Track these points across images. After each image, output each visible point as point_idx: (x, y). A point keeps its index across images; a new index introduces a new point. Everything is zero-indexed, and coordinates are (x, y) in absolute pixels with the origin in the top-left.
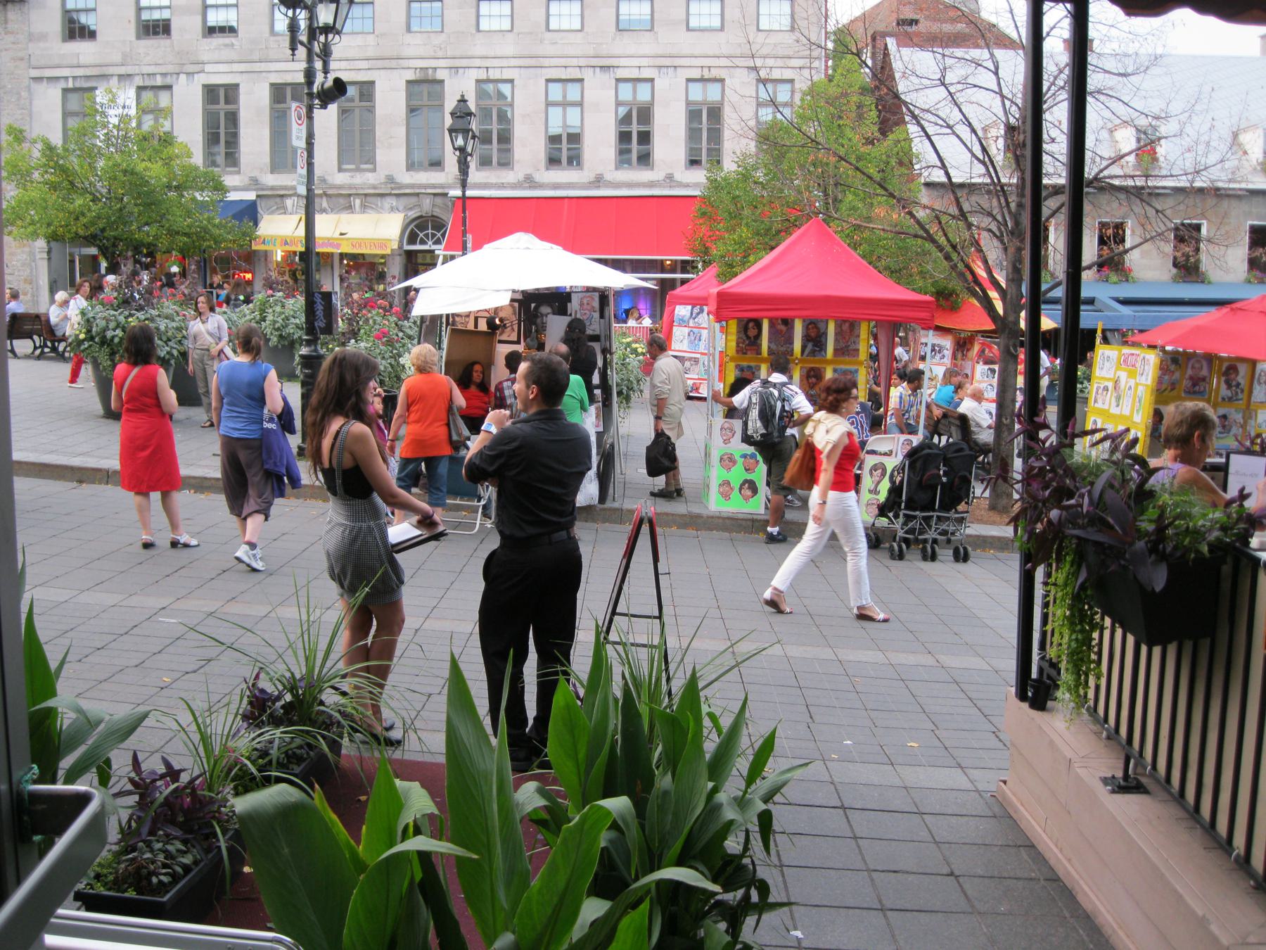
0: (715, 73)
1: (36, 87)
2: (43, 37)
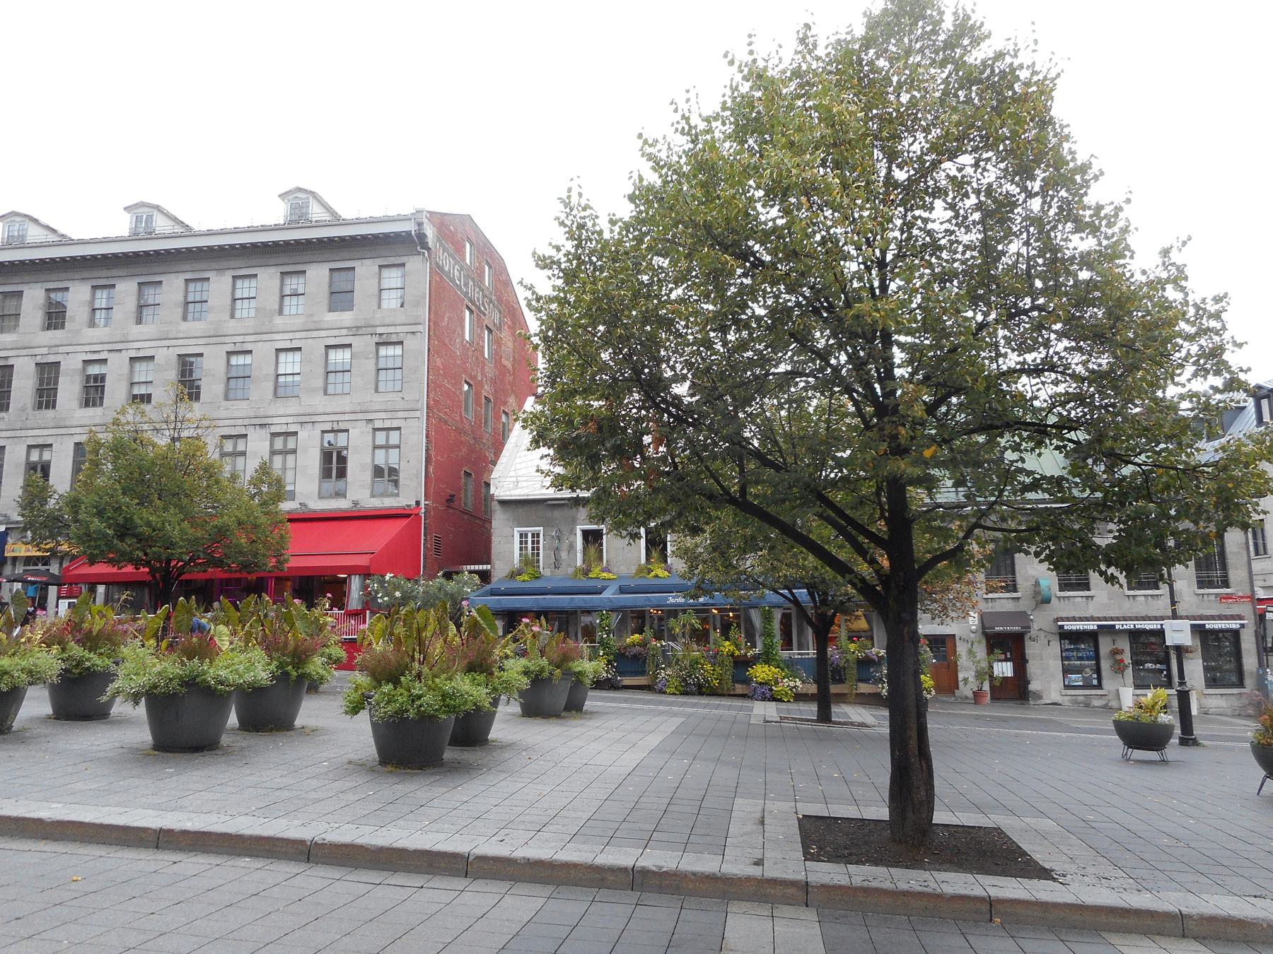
0: (342, 426)
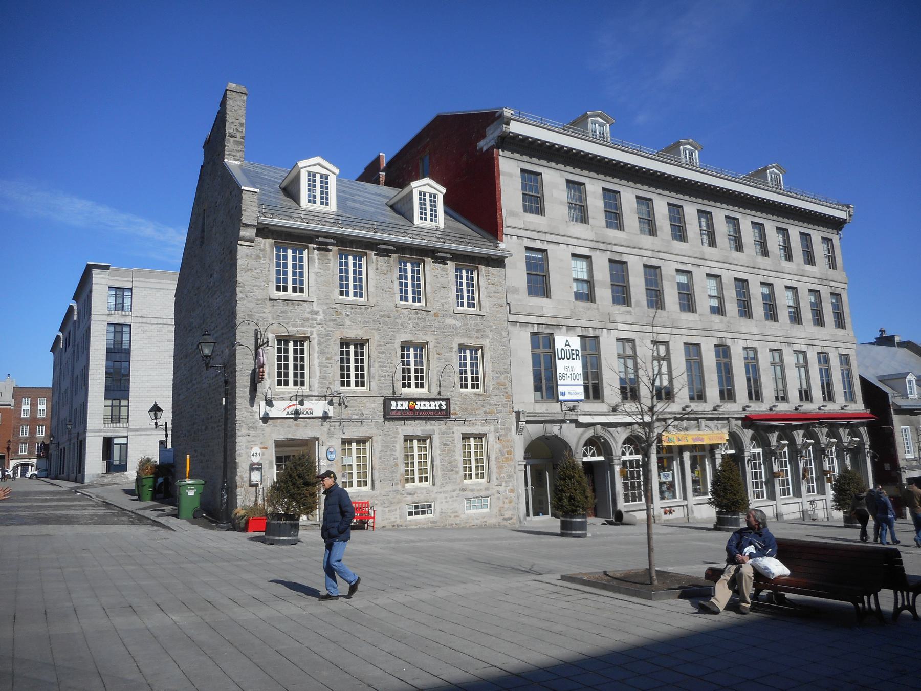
2: (516, 291)
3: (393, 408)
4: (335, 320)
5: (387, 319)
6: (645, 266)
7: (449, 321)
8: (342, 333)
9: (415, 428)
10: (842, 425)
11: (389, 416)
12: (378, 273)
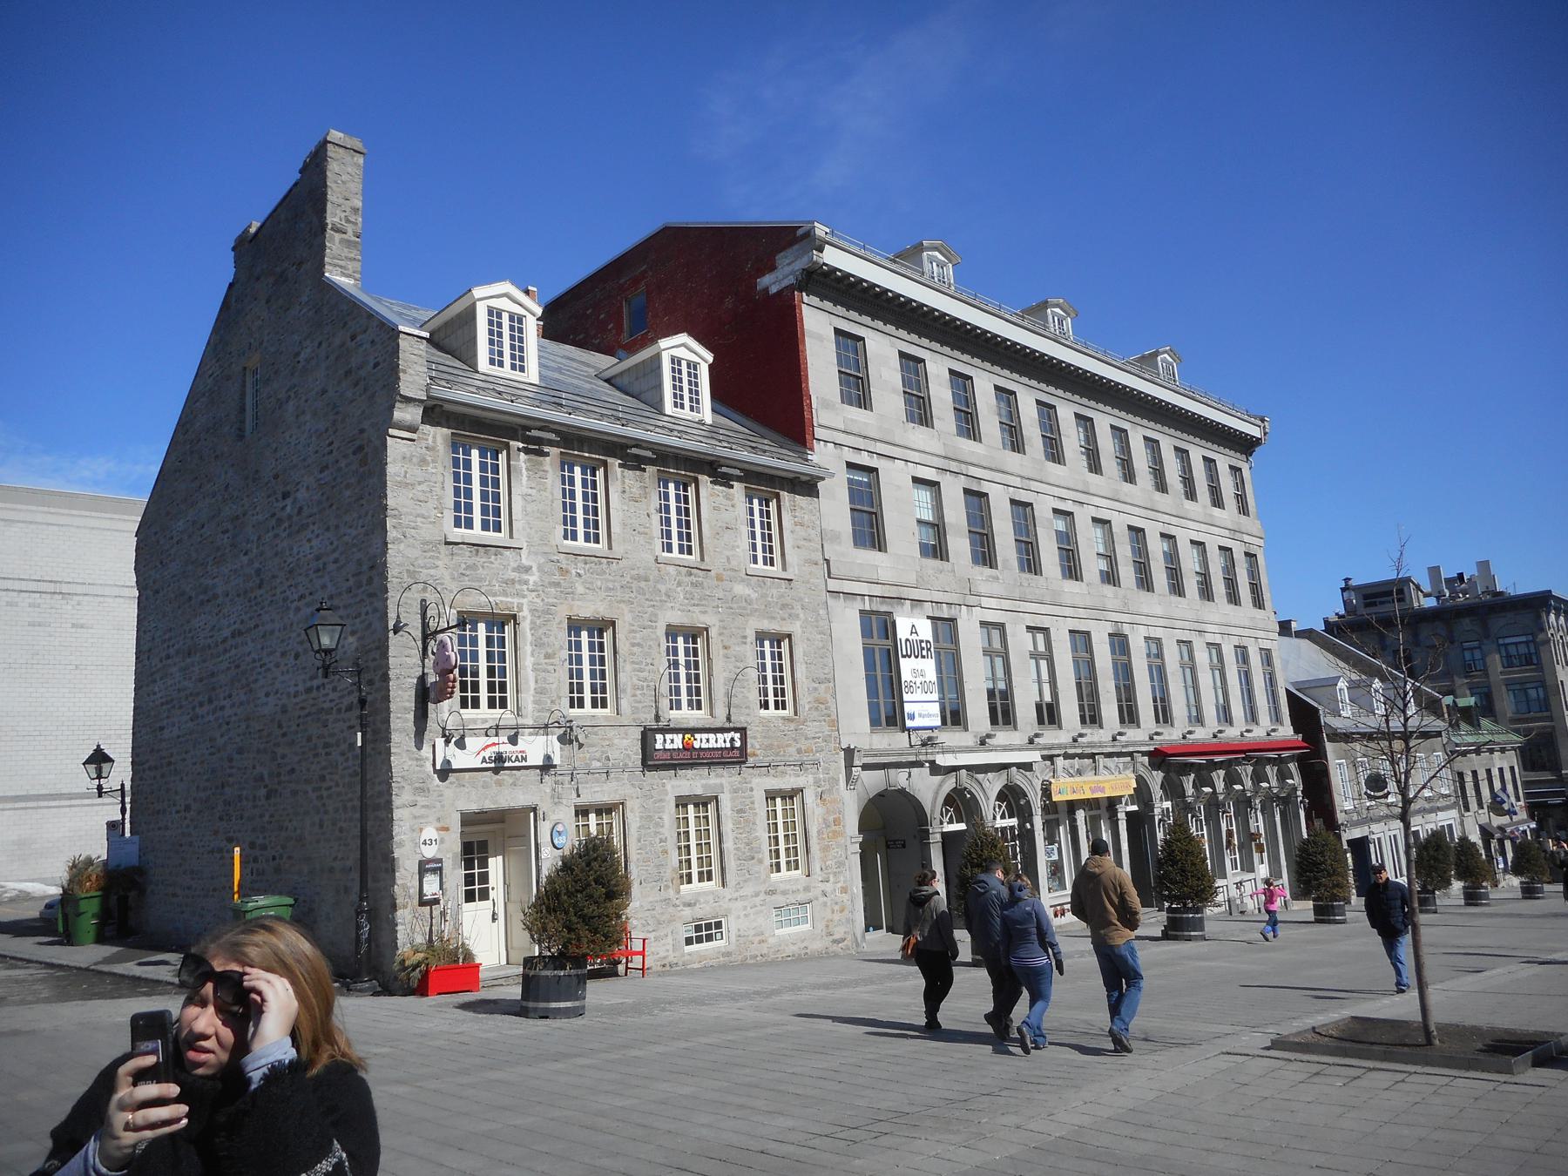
1: (837, 605)
2: (836, 538)
3: (659, 746)
4: (558, 584)
5: (643, 584)
6: (1013, 502)
7: (740, 589)
8: (571, 608)
9: (693, 782)
10: (1270, 761)
11: (651, 760)
12: (630, 497)
